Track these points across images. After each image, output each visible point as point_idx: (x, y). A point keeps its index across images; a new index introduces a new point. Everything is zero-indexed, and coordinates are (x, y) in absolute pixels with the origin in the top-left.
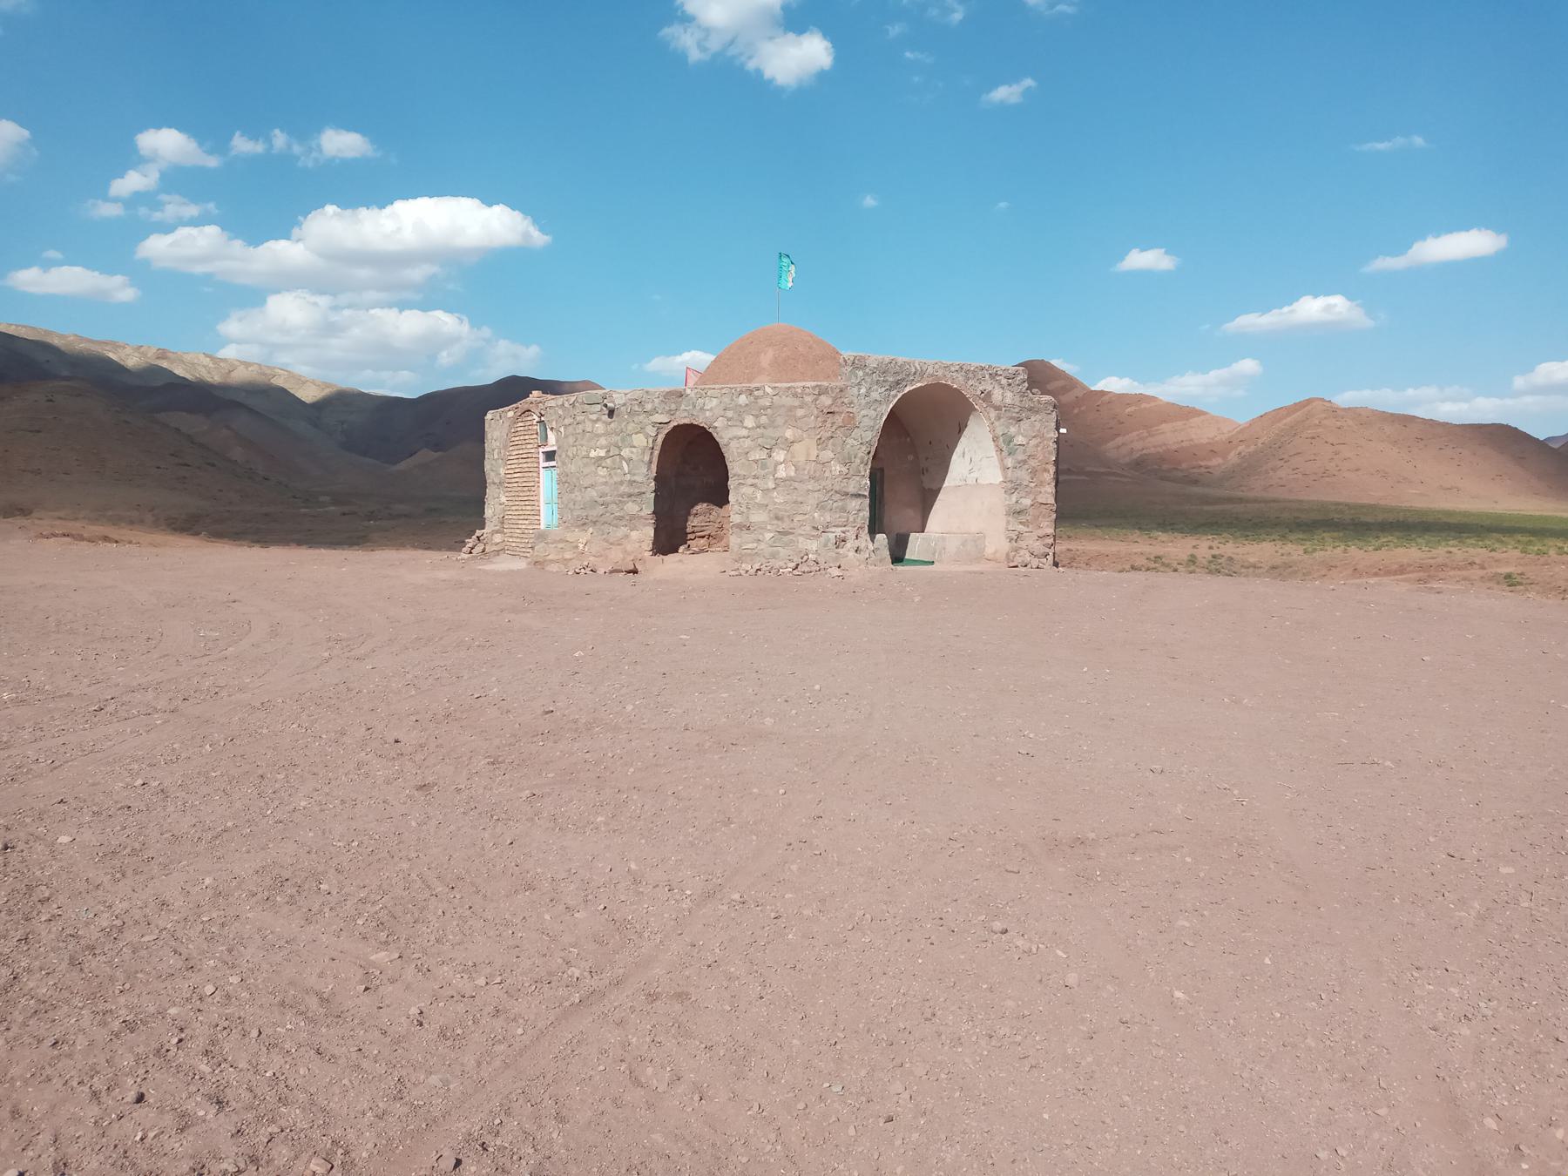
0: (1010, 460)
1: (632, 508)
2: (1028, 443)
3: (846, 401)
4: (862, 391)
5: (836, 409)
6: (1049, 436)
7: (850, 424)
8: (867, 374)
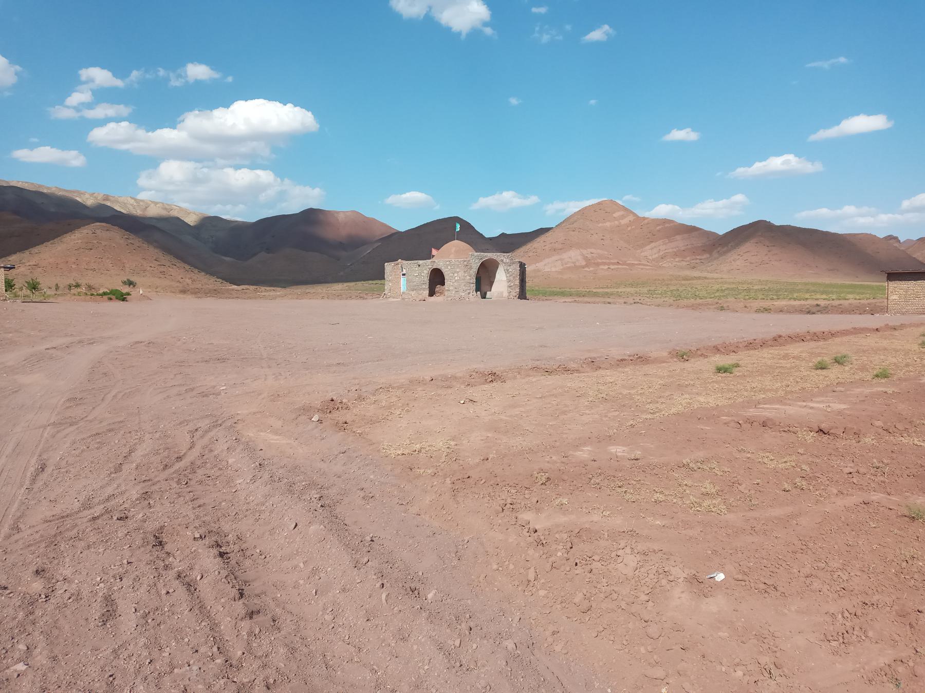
1: (424, 286)
7: (471, 268)
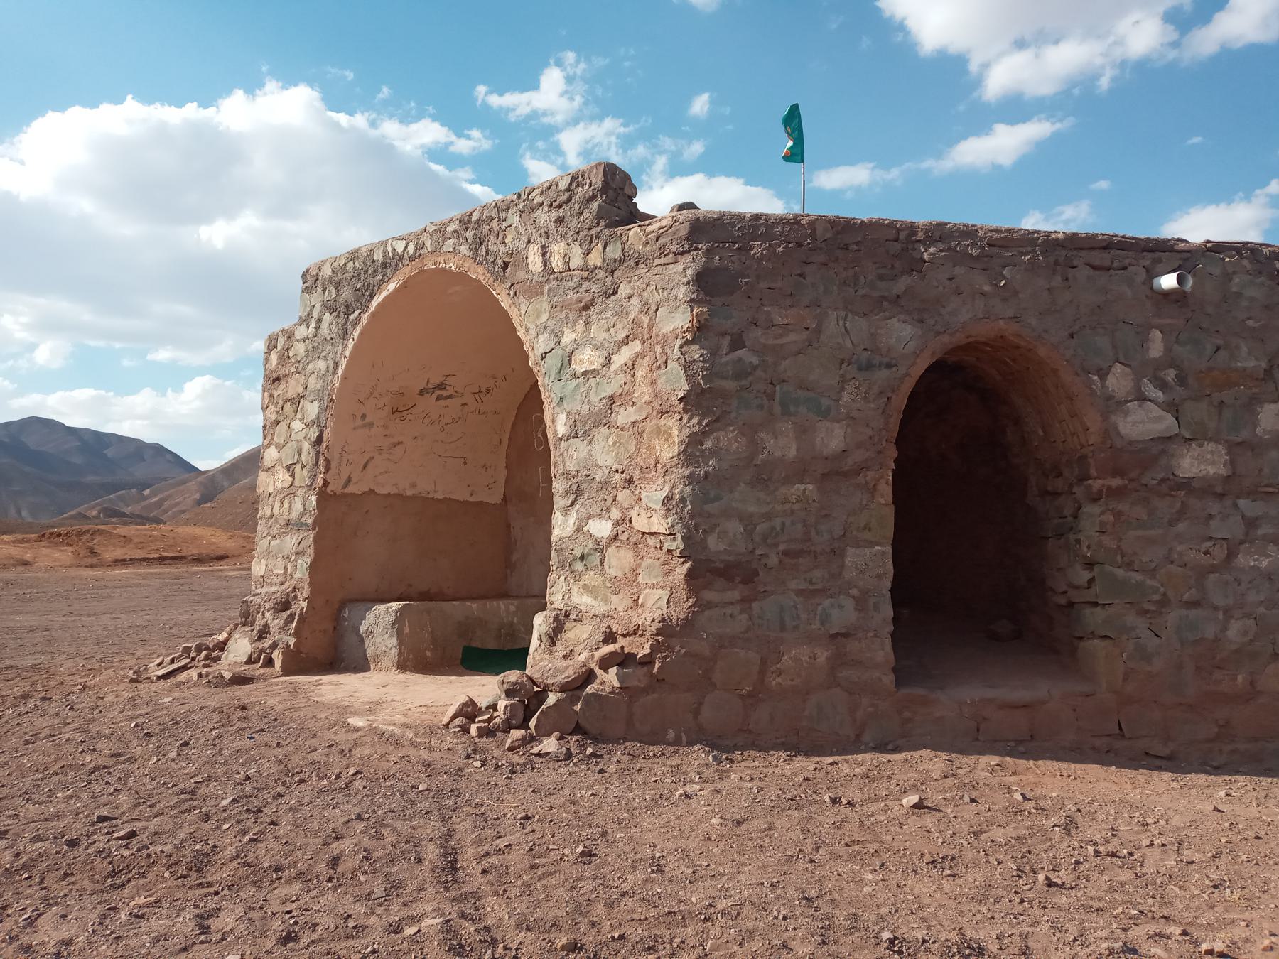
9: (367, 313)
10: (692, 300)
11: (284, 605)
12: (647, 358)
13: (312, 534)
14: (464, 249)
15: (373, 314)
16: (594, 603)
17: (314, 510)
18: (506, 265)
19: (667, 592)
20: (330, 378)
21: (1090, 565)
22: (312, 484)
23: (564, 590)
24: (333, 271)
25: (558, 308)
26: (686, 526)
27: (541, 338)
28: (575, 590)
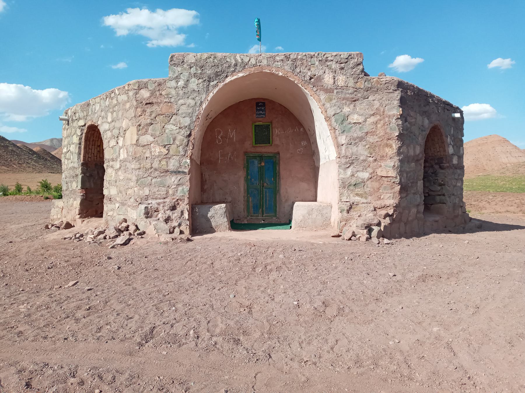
0: (344, 137)
2: (365, 121)
3: (164, 93)
4: (179, 83)
5: (154, 101)
6: (391, 113)
8: (185, 69)
9: (223, 83)
10: (399, 106)
11: (173, 208)
12: (382, 121)
13: (188, 177)
14: (287, 68)
15: (226, 84)
16: (361, 199)
17: (188, 166)
18: (311, 79)
19: (392, 194)
20: (197, 109)
21: (440, 185)
22: (185, 154)
23: (347, 195)
24: (196, 60)
25: (341, 99)
26: (399, 174)
27: (333, 108)
28: (351, 195)
